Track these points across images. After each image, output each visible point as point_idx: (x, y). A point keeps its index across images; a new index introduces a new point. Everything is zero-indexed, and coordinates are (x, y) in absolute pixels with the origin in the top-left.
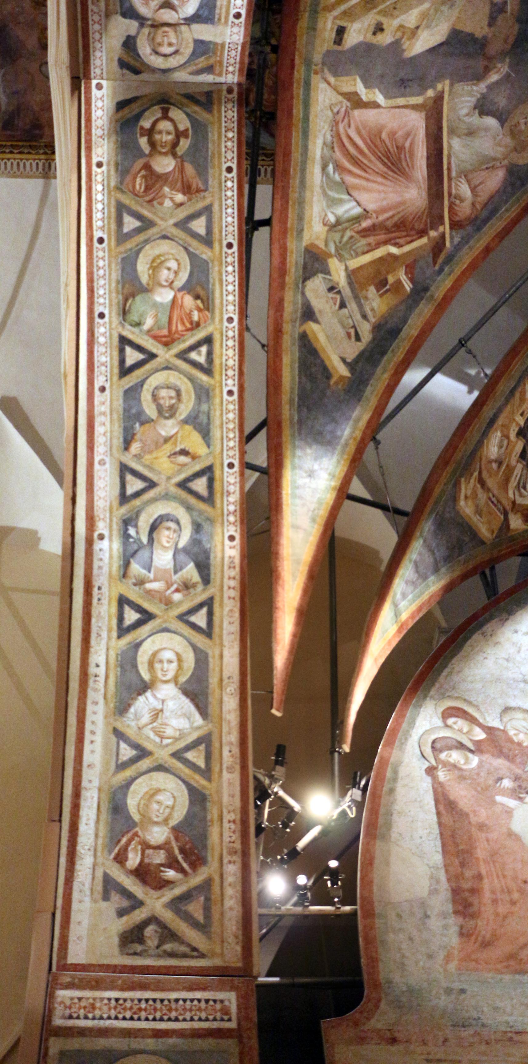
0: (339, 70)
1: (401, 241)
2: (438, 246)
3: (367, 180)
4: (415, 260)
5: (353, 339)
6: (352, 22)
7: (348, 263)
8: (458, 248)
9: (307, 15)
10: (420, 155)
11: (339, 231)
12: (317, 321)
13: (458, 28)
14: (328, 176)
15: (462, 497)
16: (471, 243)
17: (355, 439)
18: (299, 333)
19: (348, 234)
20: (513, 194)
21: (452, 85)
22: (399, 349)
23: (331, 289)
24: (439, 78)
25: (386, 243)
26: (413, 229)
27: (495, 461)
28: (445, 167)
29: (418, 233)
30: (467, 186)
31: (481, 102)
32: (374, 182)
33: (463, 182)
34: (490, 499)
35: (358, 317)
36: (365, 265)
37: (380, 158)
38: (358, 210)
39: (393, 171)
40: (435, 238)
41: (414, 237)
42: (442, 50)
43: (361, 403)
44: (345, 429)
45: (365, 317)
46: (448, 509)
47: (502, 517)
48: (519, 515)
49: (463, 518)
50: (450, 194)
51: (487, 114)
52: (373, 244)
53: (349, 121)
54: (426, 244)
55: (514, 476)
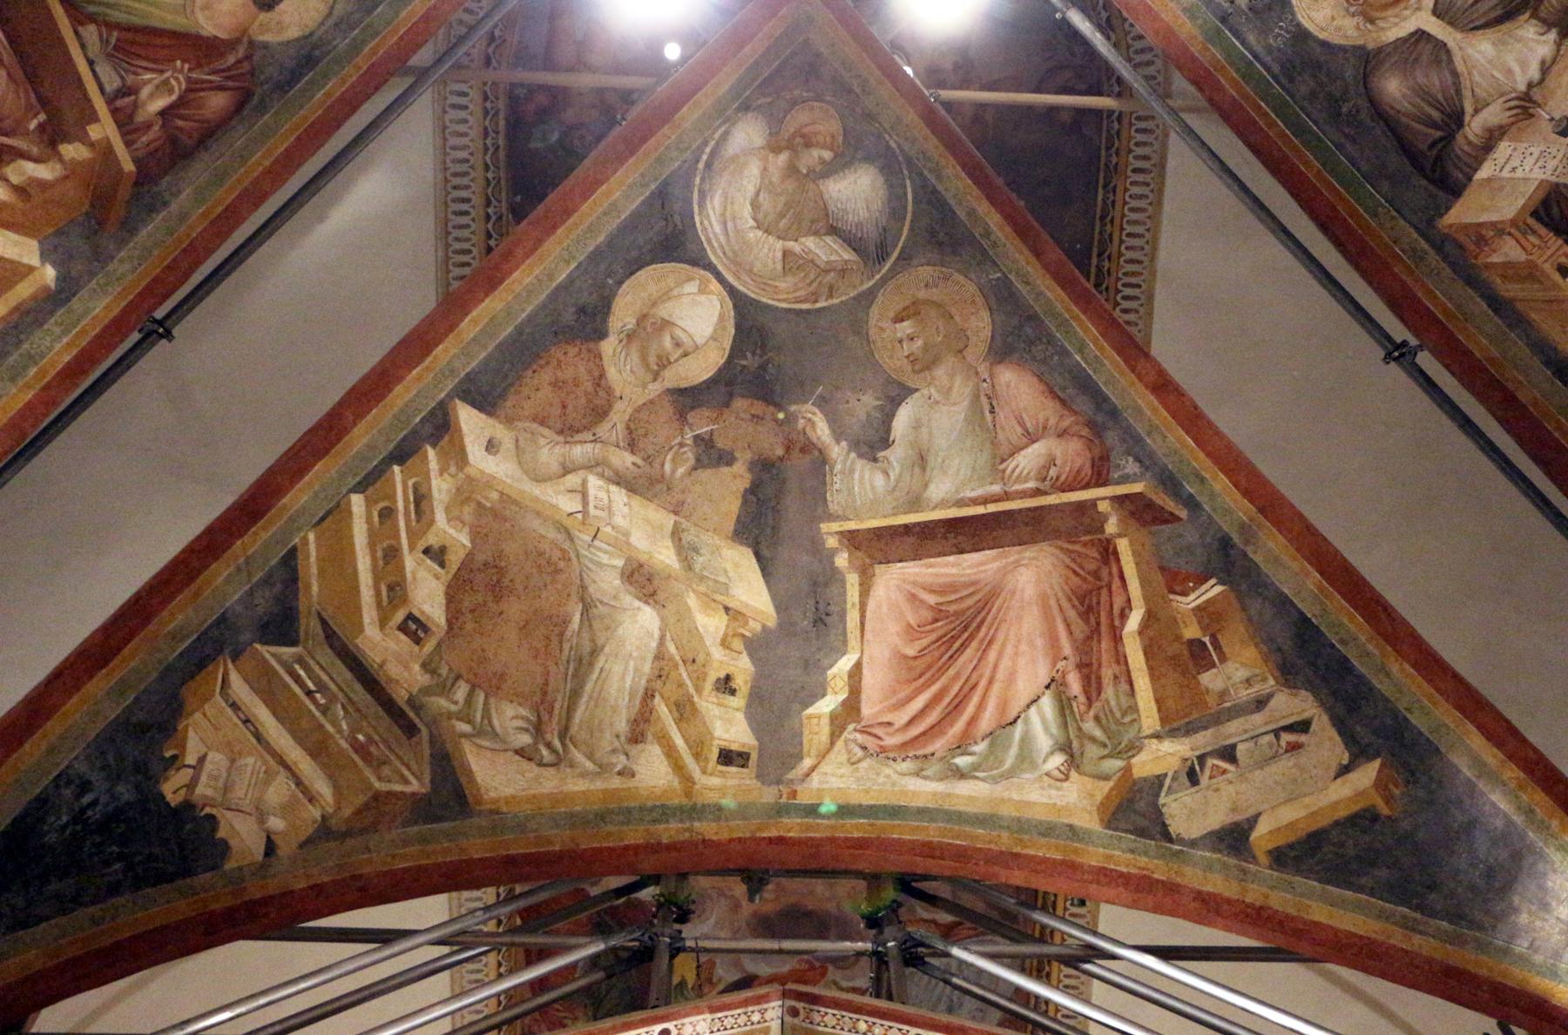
0: (791, 750)
1: (1118, 602)
2: (1139, 511)
3: (991, 682)
4: (1162, 569)
5: (1303, 738)
6: (713, 738)
7: (1148, 732)
8: (1147, 461)
9: (697, 824)
10: (954, 571)
11: (1082, 746)
12: (1253, 821)
13: (730, 525)
14: (976, 767)
16: (1140, 429)
17: (1521, 787)
18: (1271, 868)
19: (1090, 726)
20: (1051, 340)
21: (832, 518)
22: (1341, 624)
23: (1193, 778)
24: (816, 546)
25: (1117, 638)
26: (1096, 574)
28: (980, 510)
29: (1106, 561)
30: (1023, 453)
31: (865, 449)
32: (996, 667)
33: (1014, 463)
35: (1257, 718)
36: (1155, 691)
37: (951, 657)
38: (1047, 703)
39: (979, 627)
40: (1120, 520)
41: (1115, 570)
42: (765, 552)
43: (1443, 750)
44: (1494, 805)
45: (1261, 703)
50: (1037, 492)
51: (888, 431)
52: (1117, 669)
53: (881, 724)
54: (1131, 543)
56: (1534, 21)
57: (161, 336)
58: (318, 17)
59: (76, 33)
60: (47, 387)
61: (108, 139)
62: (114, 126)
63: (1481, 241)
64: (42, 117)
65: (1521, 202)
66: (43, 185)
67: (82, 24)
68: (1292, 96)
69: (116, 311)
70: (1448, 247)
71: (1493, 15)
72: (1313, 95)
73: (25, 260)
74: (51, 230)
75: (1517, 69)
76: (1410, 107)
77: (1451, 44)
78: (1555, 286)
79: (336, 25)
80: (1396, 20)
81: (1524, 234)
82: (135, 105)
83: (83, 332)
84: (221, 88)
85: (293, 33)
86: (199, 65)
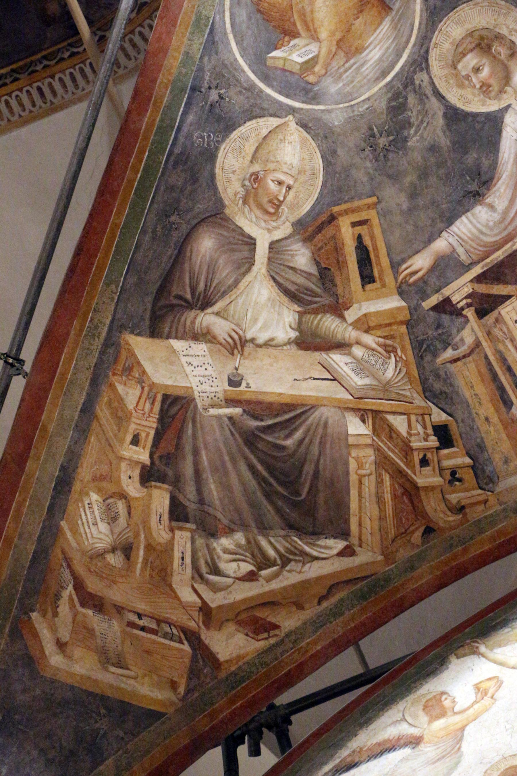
15: (49, 647)
27: (113, 550)
34: (131, 625)
46: (18, 687)
47: (186, 647)
48: (231, 627)
49: (72, 687)
55: (176, 562)
56: (297, 316)
63: (128, 370)
65: (169, 382)
68: (163, 174)
70: (111, 351)
71: (290, 286)
72: (172, 188)
75: (259, 324)
76: (198, 265)
77: (255, 268)
78: (122, 441)
80: (254, 219)
81: (148, 397)
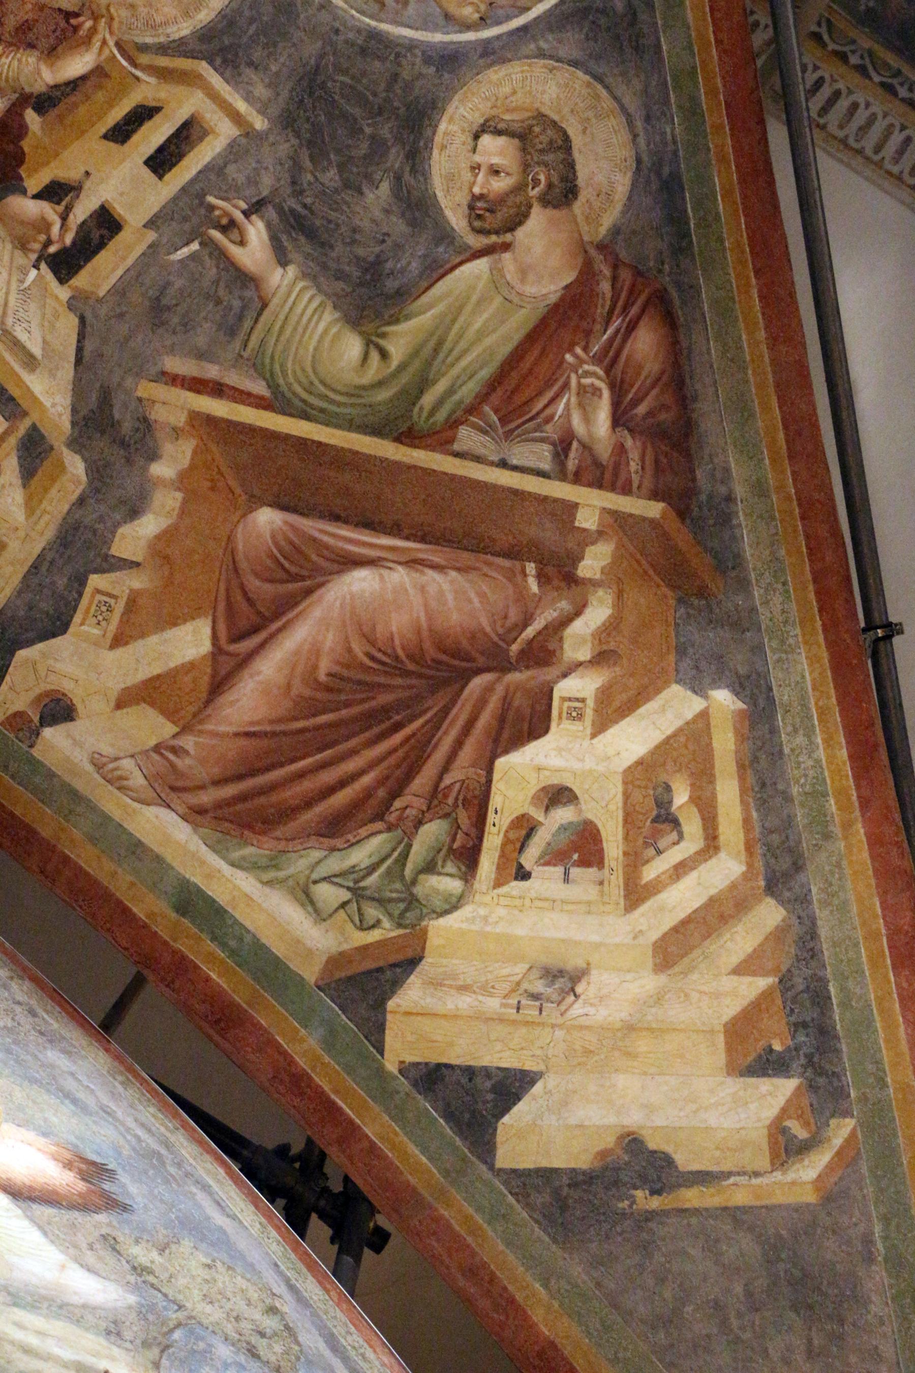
57: (888, 638)
58: (624, 136)
59: (457, 455)
60: (865, 803)
61: (604, 510)
62: (596, 492)
64: (531, 568)
66: (610, 628)
67: (451, 441)
69: (825, 655)
73: (689, 715)
74: (672, 658)
79: (648, 119)
82: (586, 447)
83: (822, 712)
84: (631, 328)
85: (622, 184)
86: (588, 333)
